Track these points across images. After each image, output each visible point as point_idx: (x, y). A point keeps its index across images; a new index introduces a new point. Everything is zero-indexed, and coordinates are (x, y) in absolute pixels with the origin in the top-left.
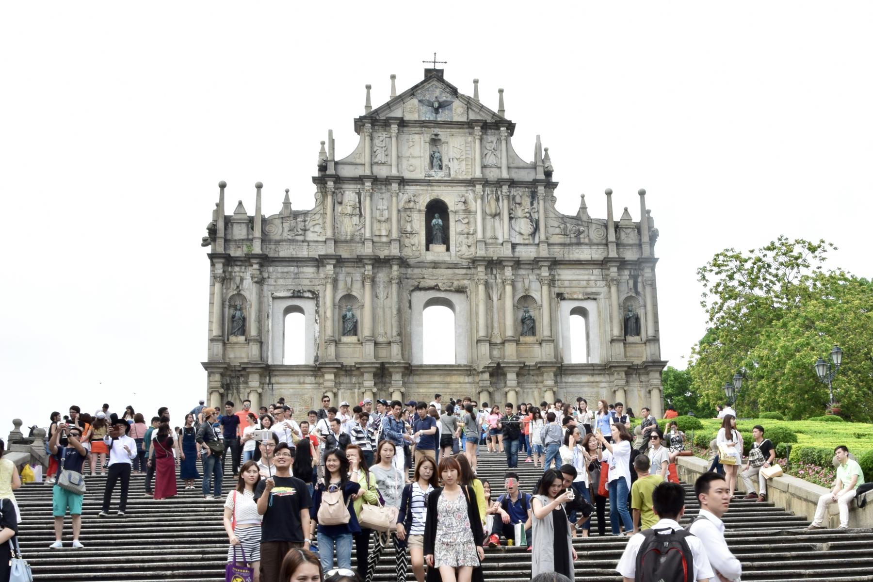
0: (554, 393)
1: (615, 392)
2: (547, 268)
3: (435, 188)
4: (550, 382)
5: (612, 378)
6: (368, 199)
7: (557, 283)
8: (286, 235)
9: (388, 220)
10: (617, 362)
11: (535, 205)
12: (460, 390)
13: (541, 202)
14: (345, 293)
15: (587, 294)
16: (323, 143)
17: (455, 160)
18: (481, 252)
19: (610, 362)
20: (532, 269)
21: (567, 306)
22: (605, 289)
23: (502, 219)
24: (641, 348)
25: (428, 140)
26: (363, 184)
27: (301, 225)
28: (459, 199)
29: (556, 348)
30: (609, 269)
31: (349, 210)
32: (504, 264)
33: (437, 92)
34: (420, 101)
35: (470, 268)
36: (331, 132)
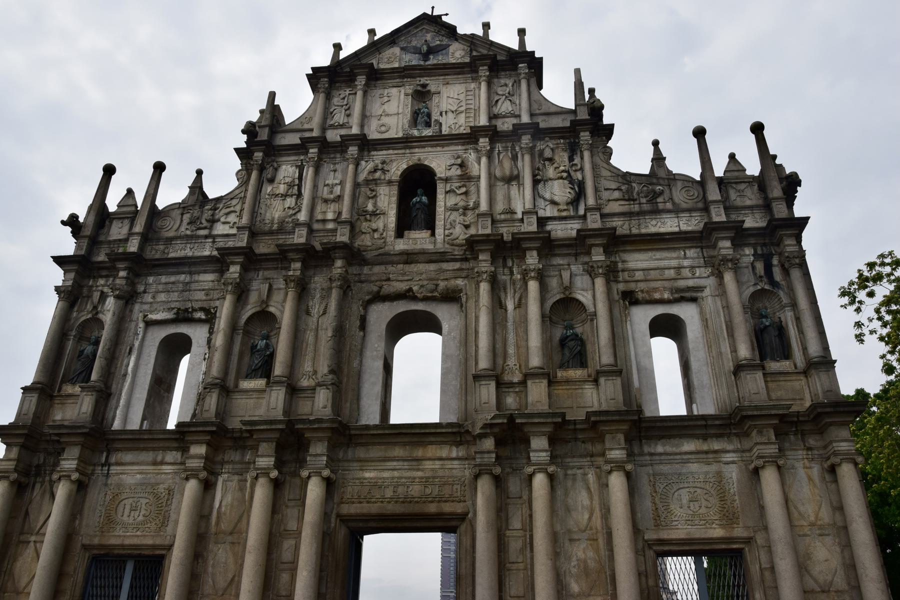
0: (628, 475)
1: (756, 471)
2: (601, 250)
3: (417, 150)
4: (617, 454)
5: (747, 444)
7: (621, 277)
8: (185, 230)
9: (339, 198)
10: (756, 408)
11: (577, 160)
12: (440, 473)
13: (587, 154)
14: (258, 309)
15: (679, 290)
16: (262, 112)
17: (450, 114)
18: (484, 229)
19: (740, 409)
20: (576, 255)
21: (642, 316)
22: (711, 282)
23: (520, 185)
24: (800, 383)
25: (411, 91)
26: (307, 153)
27: (207, 215)
28: (453, 161)
29: (627, 387)
30: (714, 246)
31: (282, 189)
32: (525, 245)
33: (429, 37)
34: (402, 49)
35: (466, 260)
36: (272, 95)
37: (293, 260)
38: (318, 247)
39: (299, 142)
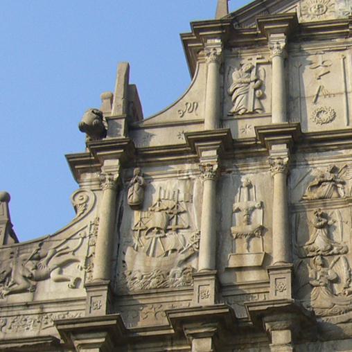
6: (207, 187)
9: (262, 230)
37: (196, 336)
38: (242, 314)
39: (183, 141)
